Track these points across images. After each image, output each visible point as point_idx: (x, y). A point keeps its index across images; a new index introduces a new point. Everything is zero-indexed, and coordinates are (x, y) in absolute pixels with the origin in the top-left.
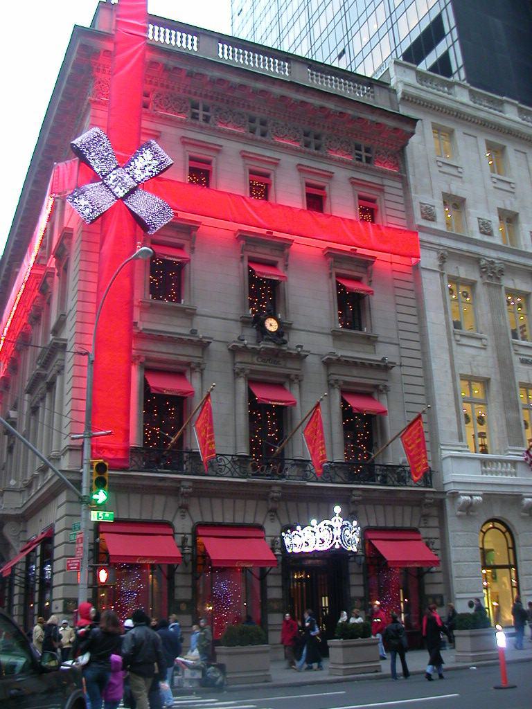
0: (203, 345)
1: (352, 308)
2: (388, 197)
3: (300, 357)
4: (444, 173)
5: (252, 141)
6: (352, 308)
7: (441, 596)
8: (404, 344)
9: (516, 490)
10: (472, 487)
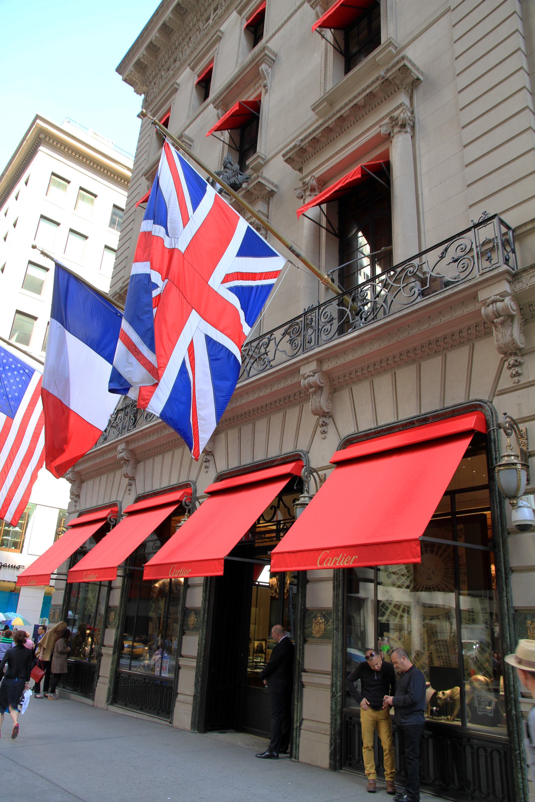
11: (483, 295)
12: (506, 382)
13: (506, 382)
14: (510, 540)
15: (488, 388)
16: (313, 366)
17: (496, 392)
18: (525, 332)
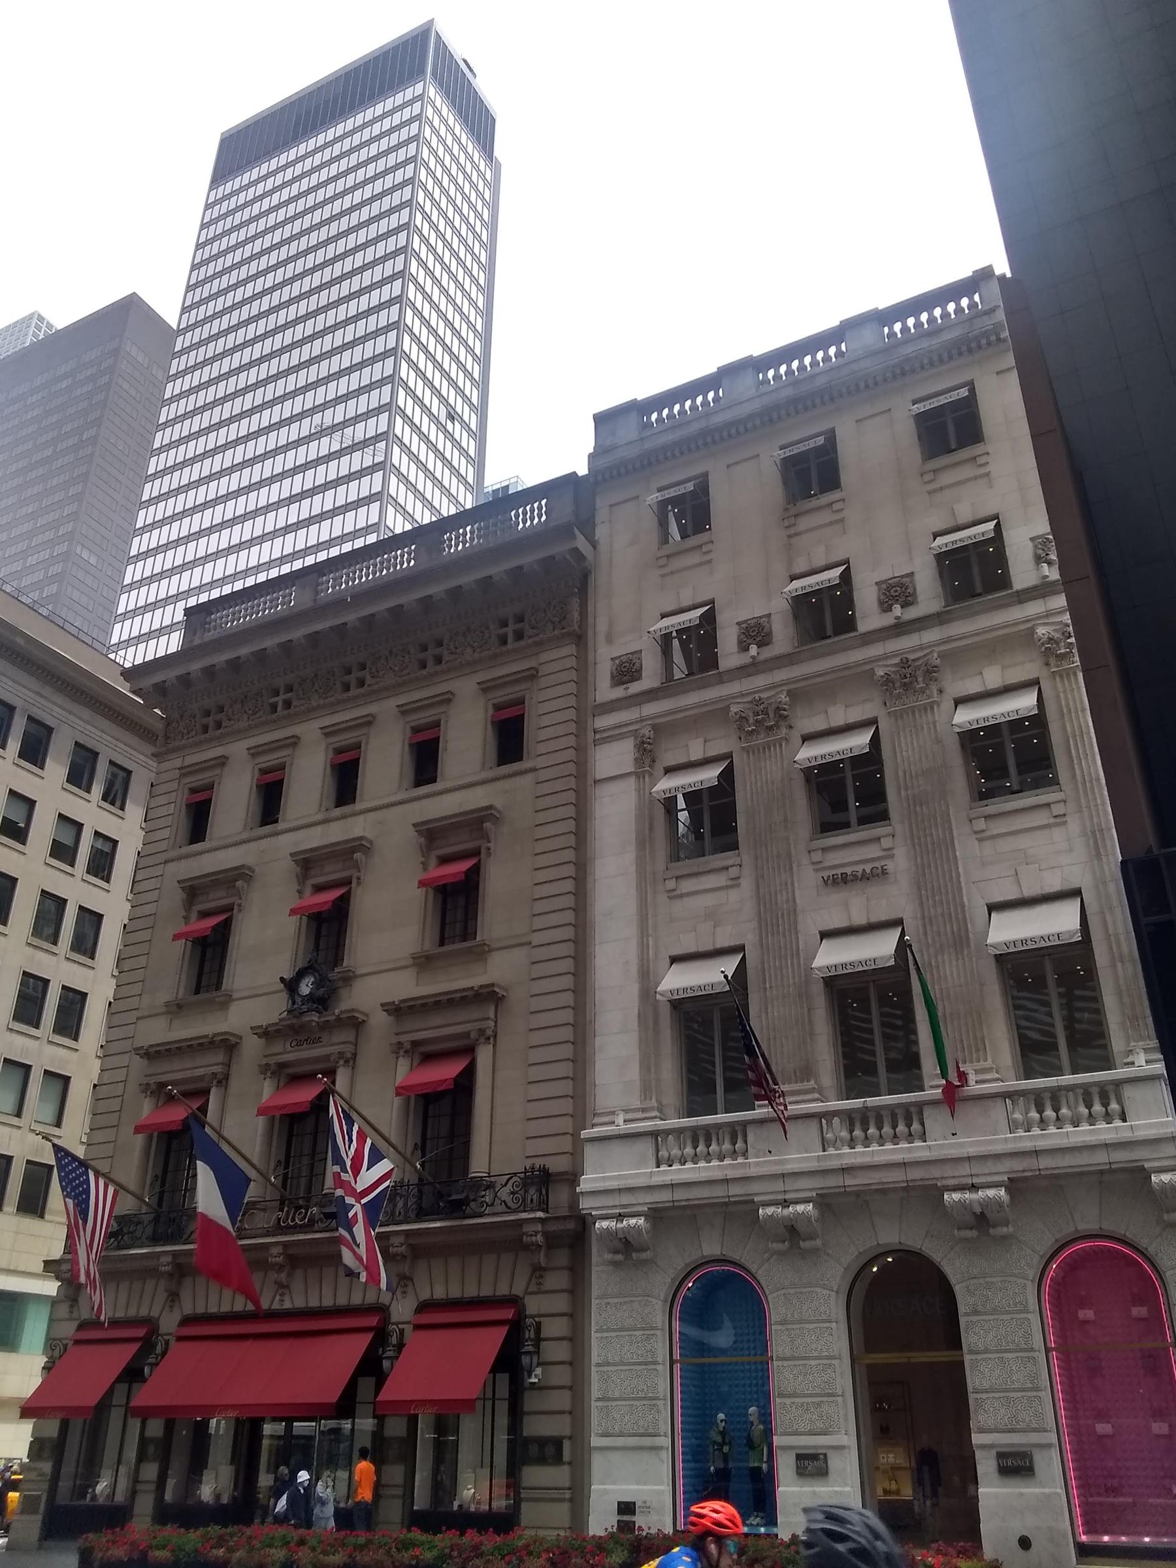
0: (228, 1045)
1: (456, 904)
2: (543, 682)
3: (356, 1023)
4: (672, 573)
6: (456, 904)
7: (558, 1443)
8: (537, 939)
9: (735, 1190)
10: (626, 1199)
14: (527, 1394)
16: (401, 1239)
17: (527, 1293)
18: (546, 1256)
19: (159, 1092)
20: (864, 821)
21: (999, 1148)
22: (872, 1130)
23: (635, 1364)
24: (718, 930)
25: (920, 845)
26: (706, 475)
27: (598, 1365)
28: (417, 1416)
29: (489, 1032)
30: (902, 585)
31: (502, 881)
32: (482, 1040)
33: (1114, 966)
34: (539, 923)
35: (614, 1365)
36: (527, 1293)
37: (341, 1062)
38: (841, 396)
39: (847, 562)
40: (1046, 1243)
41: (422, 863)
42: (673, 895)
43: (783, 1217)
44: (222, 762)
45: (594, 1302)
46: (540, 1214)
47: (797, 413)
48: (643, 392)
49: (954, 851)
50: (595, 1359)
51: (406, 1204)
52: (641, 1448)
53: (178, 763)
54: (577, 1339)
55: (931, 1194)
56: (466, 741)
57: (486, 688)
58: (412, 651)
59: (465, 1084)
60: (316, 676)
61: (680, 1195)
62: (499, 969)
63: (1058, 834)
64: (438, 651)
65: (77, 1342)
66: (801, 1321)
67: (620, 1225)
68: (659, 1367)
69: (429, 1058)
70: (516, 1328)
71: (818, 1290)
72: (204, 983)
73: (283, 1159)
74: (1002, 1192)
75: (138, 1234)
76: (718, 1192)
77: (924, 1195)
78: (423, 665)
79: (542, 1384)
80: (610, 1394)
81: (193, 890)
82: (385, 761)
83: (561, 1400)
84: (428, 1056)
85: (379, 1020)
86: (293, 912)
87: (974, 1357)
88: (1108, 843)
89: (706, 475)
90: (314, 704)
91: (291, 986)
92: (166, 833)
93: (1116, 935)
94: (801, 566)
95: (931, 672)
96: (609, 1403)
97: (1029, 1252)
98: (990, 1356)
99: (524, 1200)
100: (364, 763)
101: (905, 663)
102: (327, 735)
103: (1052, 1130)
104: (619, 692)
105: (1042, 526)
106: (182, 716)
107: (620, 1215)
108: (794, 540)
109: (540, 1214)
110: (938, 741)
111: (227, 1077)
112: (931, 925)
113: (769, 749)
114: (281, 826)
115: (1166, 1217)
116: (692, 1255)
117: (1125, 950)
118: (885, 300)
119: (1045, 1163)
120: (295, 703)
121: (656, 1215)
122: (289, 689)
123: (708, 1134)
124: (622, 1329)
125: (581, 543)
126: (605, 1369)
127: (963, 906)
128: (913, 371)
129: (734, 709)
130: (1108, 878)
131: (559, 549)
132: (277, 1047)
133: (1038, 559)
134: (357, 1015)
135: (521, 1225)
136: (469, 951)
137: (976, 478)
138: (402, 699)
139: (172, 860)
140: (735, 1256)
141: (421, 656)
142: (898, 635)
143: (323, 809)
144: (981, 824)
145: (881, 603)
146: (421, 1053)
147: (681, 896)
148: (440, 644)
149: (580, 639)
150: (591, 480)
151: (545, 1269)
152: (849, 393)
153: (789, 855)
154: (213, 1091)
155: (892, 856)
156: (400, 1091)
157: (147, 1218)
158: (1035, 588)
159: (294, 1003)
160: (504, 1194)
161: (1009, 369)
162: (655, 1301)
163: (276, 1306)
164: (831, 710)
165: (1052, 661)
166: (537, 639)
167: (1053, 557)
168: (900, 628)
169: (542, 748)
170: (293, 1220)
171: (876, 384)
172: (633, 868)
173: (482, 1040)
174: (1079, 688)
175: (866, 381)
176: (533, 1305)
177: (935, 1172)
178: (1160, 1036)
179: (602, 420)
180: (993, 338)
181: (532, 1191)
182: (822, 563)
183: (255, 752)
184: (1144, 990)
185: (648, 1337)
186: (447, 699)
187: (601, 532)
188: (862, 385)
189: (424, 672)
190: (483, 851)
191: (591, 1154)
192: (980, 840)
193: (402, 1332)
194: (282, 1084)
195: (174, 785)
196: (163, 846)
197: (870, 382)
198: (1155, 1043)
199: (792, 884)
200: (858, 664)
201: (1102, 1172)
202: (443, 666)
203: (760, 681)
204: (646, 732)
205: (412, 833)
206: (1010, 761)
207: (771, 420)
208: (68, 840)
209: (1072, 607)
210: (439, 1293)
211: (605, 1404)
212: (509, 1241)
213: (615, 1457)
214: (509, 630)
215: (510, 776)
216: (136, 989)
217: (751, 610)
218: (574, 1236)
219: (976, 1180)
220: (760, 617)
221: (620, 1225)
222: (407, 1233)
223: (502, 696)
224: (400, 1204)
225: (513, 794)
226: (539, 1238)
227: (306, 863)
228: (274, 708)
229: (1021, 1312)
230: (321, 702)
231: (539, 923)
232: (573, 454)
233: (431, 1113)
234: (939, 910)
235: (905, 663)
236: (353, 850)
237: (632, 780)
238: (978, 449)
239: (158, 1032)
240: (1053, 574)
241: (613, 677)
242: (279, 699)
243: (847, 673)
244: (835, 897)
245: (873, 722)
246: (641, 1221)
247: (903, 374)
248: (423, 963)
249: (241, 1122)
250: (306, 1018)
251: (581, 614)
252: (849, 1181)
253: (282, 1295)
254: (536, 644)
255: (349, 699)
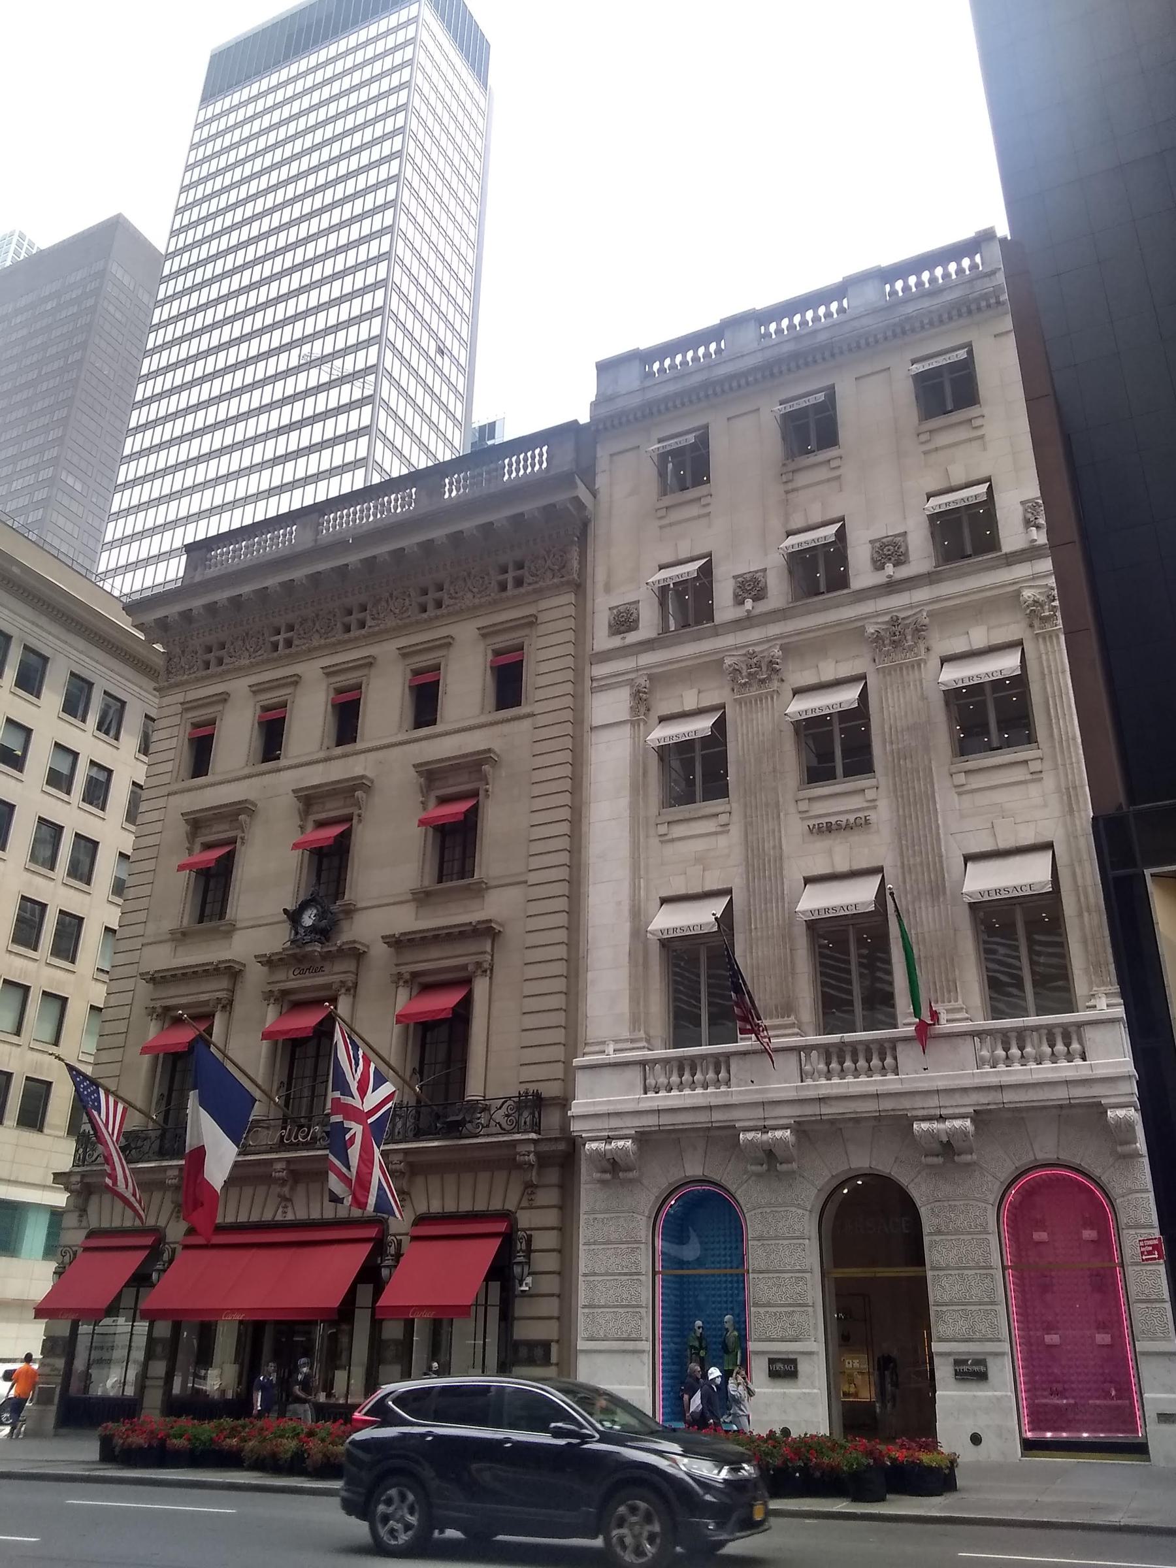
0: (232, 972)
1: (455, 843)
2: (542, 629)
3: (357, 954)
4: (671, 525)
5: (334, 648)
6: (455, 843)
7: (546, 1345)
8: (533, 878)
9: (717, 1116)
10: (615, 1123)
11: (521, 1149)
12: (524, 1204)
13: (524, 1204)
14: (517, 1300)
15: (516, 1203)
16: (400, 1157)
17: (519, 1208)
18: (538, 1174)
19: (168, 1016)
20: (850, 772)
21: (967, 1083)
22: (848, 1064)
23: (620, 1274)
24: (706, 873)
25: (902, 797)
26: (706, 427)
27: (585, 1275)
28: (413, 1320)
29: (486, 965)
30: (895, 544)
31: (499, 822)
32: (479, 972)
33: (1080, 915)
34: (536, 862)
35: (602, 1275)
36: (519, 1208)
37: (343, 991)
38: (842, 353)
39: (842, 519)
40: (1006, 1170)
41: (422, 803)
42: (665, 840)
43: (762, 1142)
44: (224, 698)
45: (583, 1217)
46: (533, 1136)
47: (798, 367)
48: (646, 342)
49: (935, 803)
50: (582, 1269)
51: (405, 1124)
52: (625, 1351)
53: (180, 698)
54: (566, 1251)
55: (900, 1124)
56: (466, 684)
57: (485, 634)
58: (413, 594)
59: (462, 1015)
60: (317, 615)
61: (666, 1120)
62: (496, 906)
63: (1034, 790)
64: (438, 595)
65: (86, 1249)
66: (776, 1238)
67: (608, 1147)
68: (642, 1278)
69: (428, 988)
70: (508, 1240)
71: (793, 1209)
72: (208, 911)
73: (285, 1080)
74: (968, 1123)
75: (146, 1148)
76: (702, 1118)
77: (894, 1125)
78: (424, 609)
79: (532, 1292)
80: (596, 1302)
81: (196, 823)
82: (385, 703)
83: (550, 1307)
84: (426, 985)
85: (379, 952)
86: (296, 846)
87: (936, 1273)
88: (1081, 799)
89: (706, 427)
90: (315, 643)
91: (294, 917)
92: (168, 767)
93: (1085, 888)
94: (797, 522)
95: (919, 631)
96: (596, 1310)
97: (990, 1178)
98: (952, 1272)
99: (517, 1122)
100: (365, 703)
101: (895, 621)
102: (328, 675)
103: (1017, 1067)
104: (616, 642)
105: (1032, 491)
106: (183, 652)
107: (609, 1137)
108: (790, 496)
109: (533, 1136)
110: (923, 698)
111: (231, 1002)
112: (910, 872)
113: (761, 701)
114: (283, 762)
115: (1119, 1149)
116: (676, 1175)
117: (1092, 900)
118: (888, 258)
119: (1009, 1097)
120: (296, 642)
121: (643, 1138)
122: (291, 628)
123: (692, 1064)
124: (608, 1242)
125: (582, 492)
126: (592, 1278)
127: (941, 856)
128: (913, 330)
129: (728, 661)
130: (1079, 832)
131: (560, 497)
132: (280, 975)
133: (1028, 523)
134: (358, 946)
135: (515, 1147)
136: (468, 888)
137: (970, 440)
138: (403, 642)
139: (176, 793)
140: (716, 1177)
141: (423, 599)
142: (890, 593)
143: (324, 747)
144: (961, 779)
145: (874, 561)
146: (420, 984)
147: (673, 840)
148: (440, 588)
149: (579, 587)
150: (593, 428)
151: (536, 1186)
152: (850, 350)
153: (777, 804)
154: (218, 1016)
155: (875, 807)
156: (400, 1019)
157: (153, 1134)
158: (1023, 551)
159: (297, 933)
160: (499, 1116)
161: (1008, 332)
162: (640, 1217)
163: (279, 1217)
164: (822, 665)
165: (1036, 623)
166: (537, 586)
167: (1042, 521)
168: (892, 587)
169: (541, 694)
170: (296, 1138)
171: (877, 342)
172: (627, 813)
173: (479, 972)
174: (1060, 650)
175: (867, 339)
176: (525, 1219)
177: (906, 1103)
178: (1121, 982)
179: (604, 368)
180: (993, 301)
181: (526, 1114)
182: (817, 518)
183: (256, 690)
184: (1108, 939)
185: (633, 1250)
186: (447, 643)
187: (601, 481)
188: (863, 342)
189: (425, 616)
190: (482, 793)
191: (582, 1079)
192: (959, 794)
193: (400, 1242)
194: (284, 1010)
195: (177, 720)
196: (166, 779)
197: (871, 340)
198: (1116, 988)
199: (780, 831)
200: (851, 621)
201: (1061, 1107)
202: (444, 611)
203: (755, 634)
204: (643, 681)
205: (412, 772)
206: (991, 719)
207: (772, 375)
208: (65, 769)
209: (1058, 572)
210: (436, 1207)
211: (591, 1310)
212: (502, 1161)
213: (600, 1359)
214: (510, 577)
215: (508, 721)
216: (142, 916)
217: (747, 564)
218: (564, 1157)
219: (944, 1112)
220: (756, 572)
221: (608, 1147)
222: (406, 1152)
223: (502, 641)
224: (399, 1125)
225: (511, 738)
226: (532, 1157)
227: (308, 799)
228: (275, 646)
229: (980, 1233)
230: (323, 642)
231: (536, 862)
232: (574, 403)
233: (428, 1040)
234: (918, 860)
235: (895, 621)
236: (354, 789)
237: (628, 727)
238: (973, 412)
239: (163, 958)
240: (1041, 538)
241: (610, 626)
242: (280, 638)
243: (838, 629)
244: (821, 844)
245: (862, 677)
246: (629, 1143)
247: (904, 333)
248: (422, 898)
249: (245, 1048)
250: (309, 949)
251: (580, 563)
252: (826, 1110)
253: (286, 1207)
254: (535, 591)
255: (350, 640)
